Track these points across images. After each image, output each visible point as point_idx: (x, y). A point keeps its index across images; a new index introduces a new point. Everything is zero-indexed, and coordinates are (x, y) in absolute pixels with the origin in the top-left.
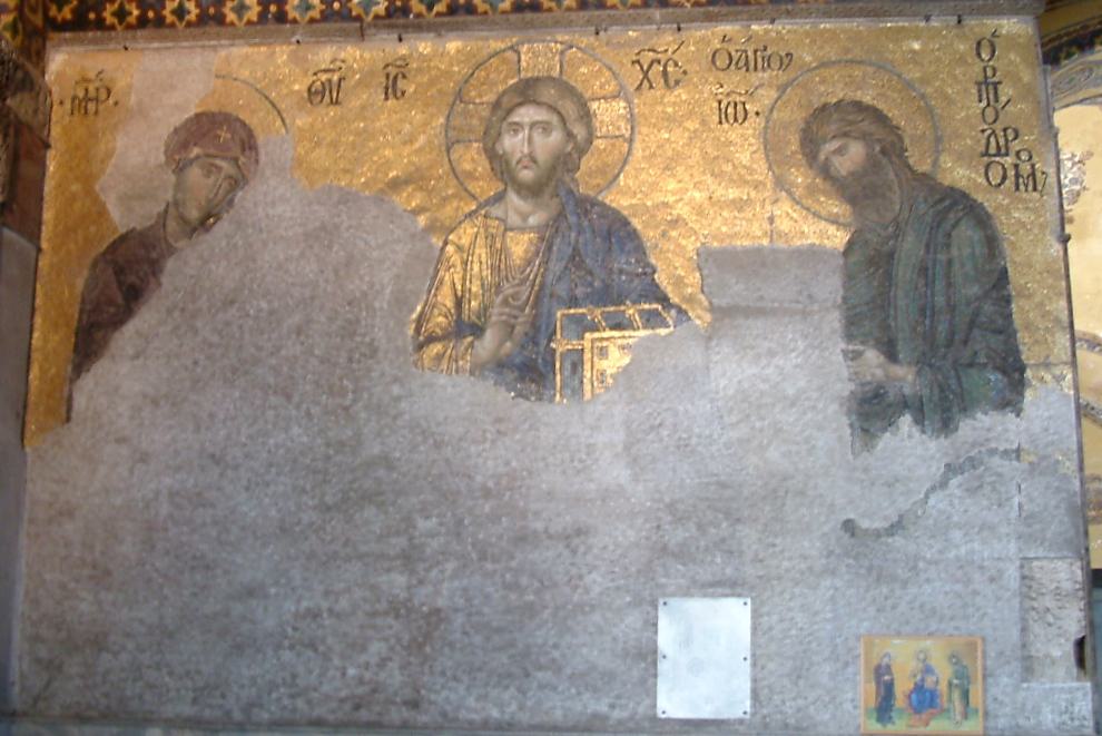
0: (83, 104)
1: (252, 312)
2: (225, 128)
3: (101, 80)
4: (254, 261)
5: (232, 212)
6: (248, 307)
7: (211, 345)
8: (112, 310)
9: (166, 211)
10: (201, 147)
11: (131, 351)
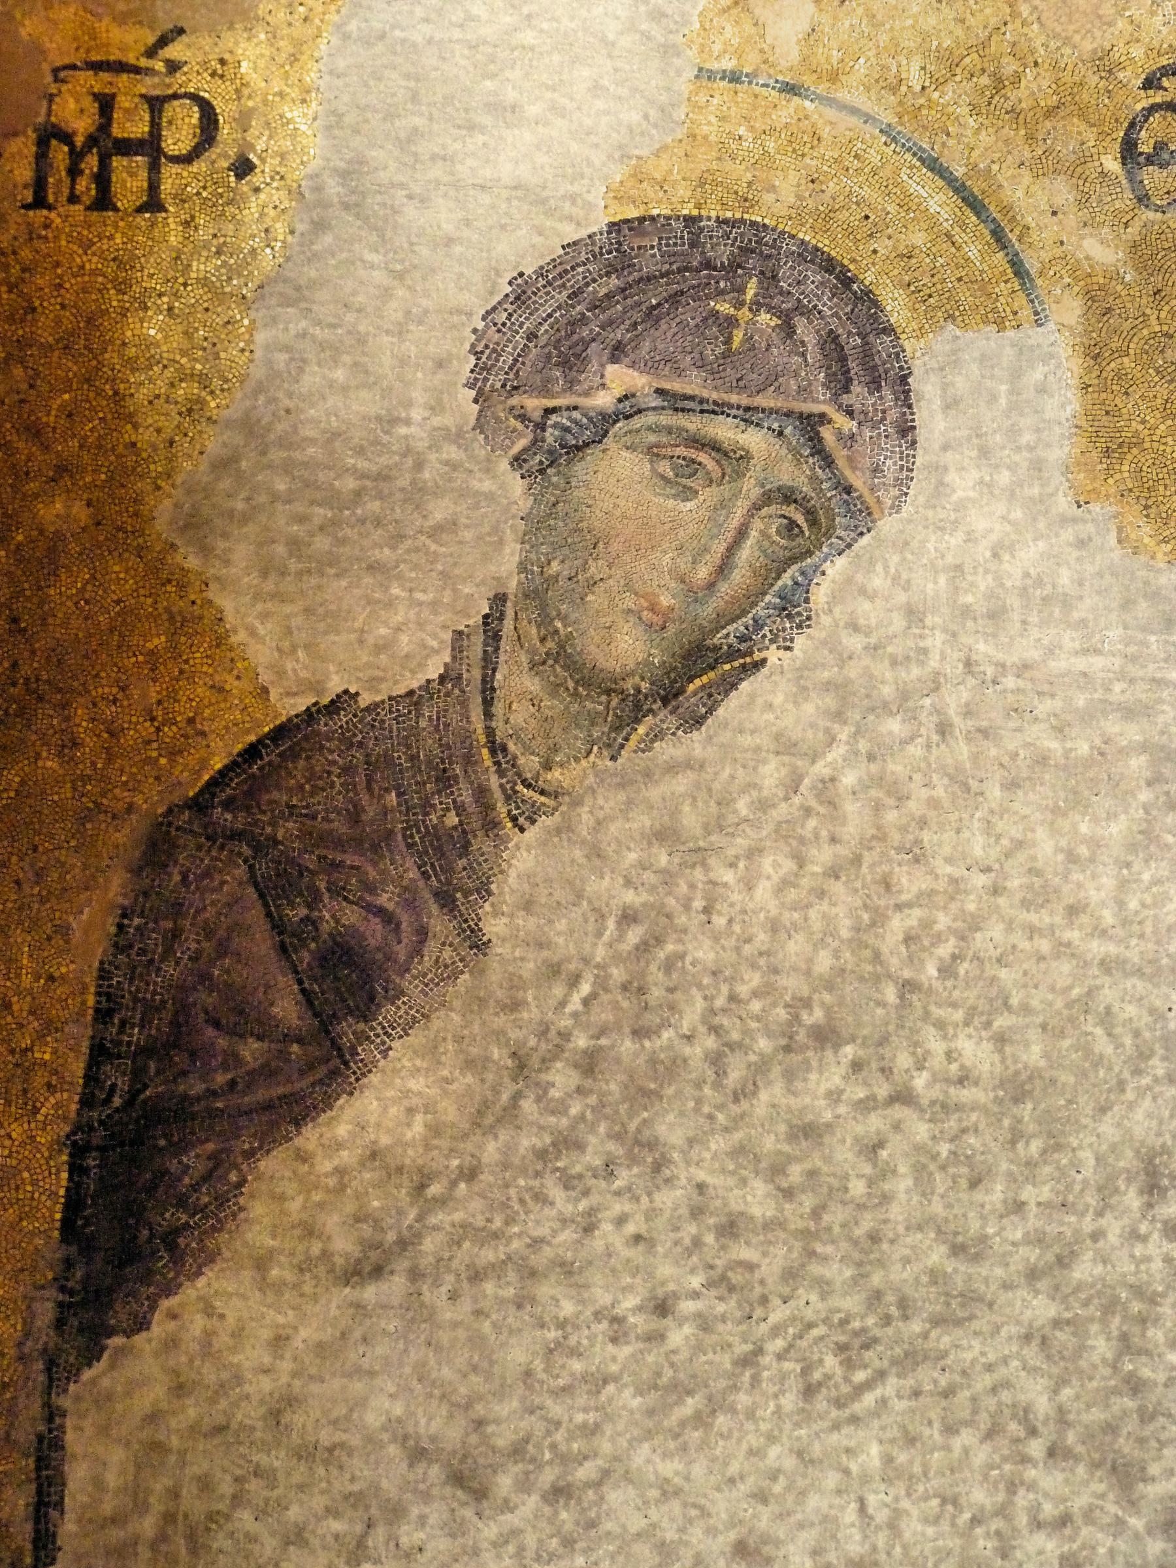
0: (91, 163)
1: (920, 1082)
2: (750, 293)
3: (173, 67)
4: (917, 856)
5: (800, 643)
6: (904, 1061)
7: (730, 1228)
8: (251, 1051)
9: (491, 625)
10: (650, 367)
11: (344, 1245)
